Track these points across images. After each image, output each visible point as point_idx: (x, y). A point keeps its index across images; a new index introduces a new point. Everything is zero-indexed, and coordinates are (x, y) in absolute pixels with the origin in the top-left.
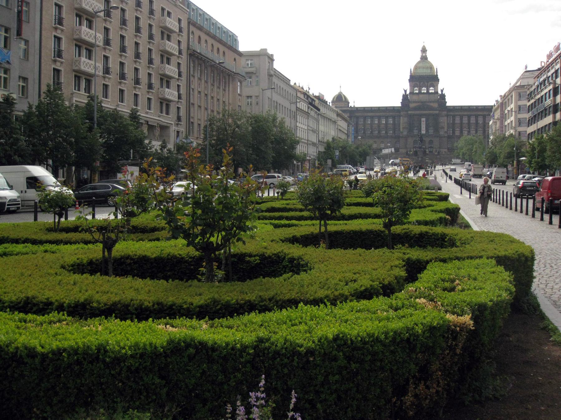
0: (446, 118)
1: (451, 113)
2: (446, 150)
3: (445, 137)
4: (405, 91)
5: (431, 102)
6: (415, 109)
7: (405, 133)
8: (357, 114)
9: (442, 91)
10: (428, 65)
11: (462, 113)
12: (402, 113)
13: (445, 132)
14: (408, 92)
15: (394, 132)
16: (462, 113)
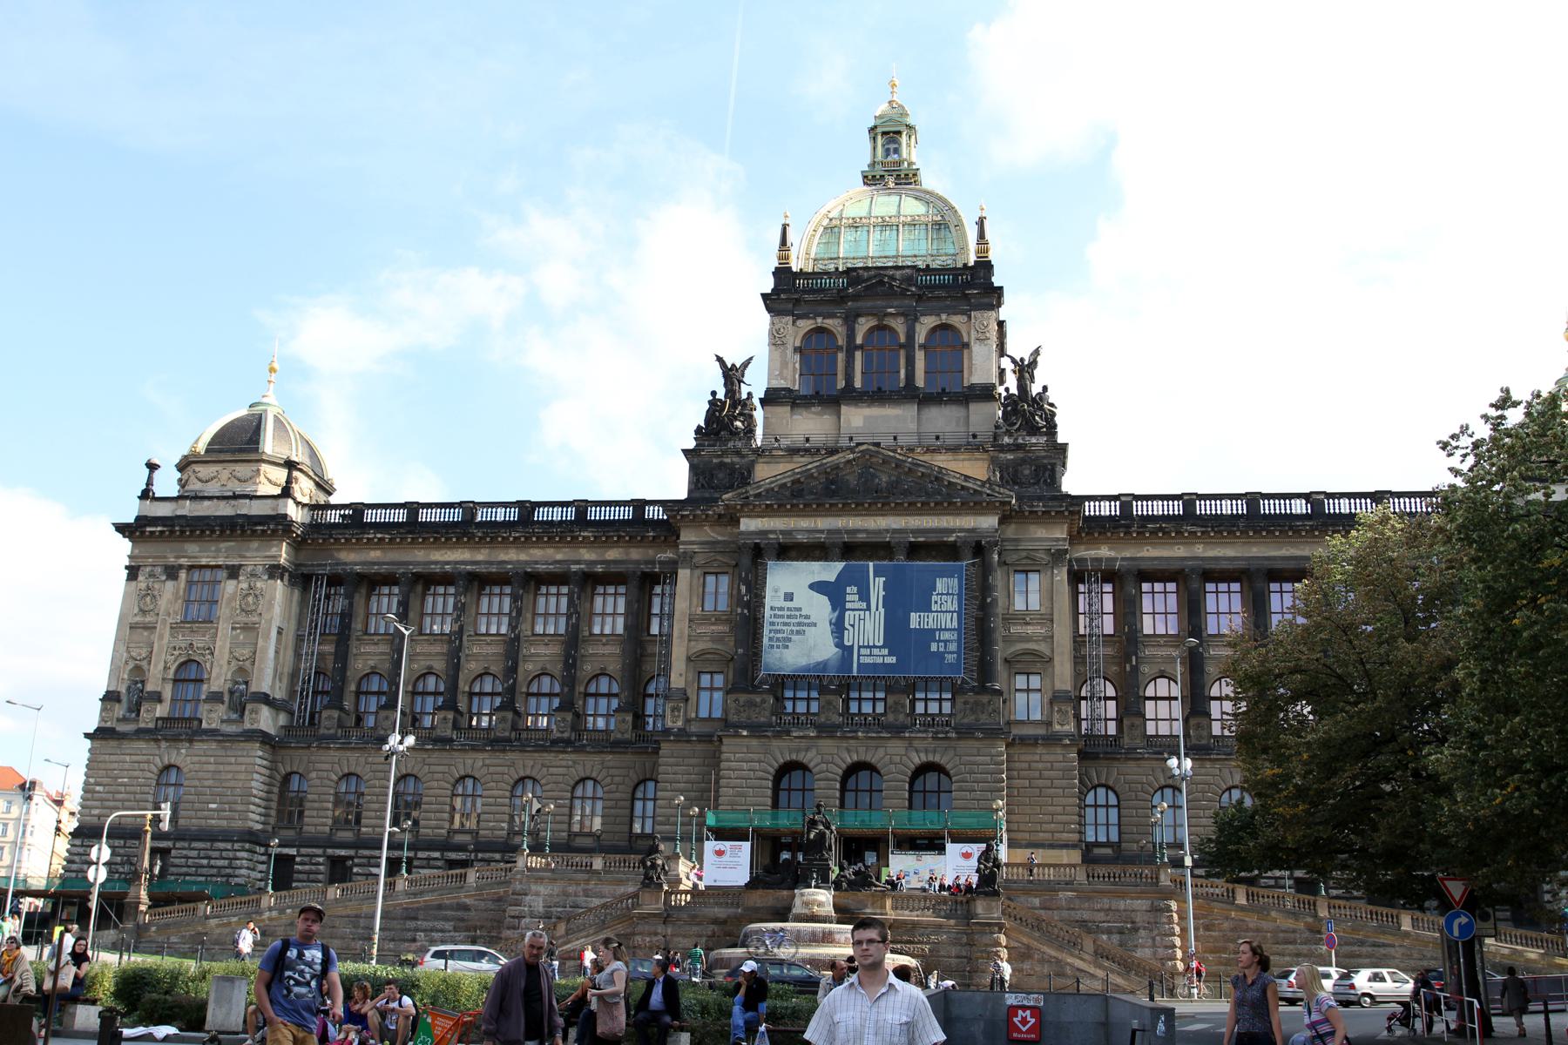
0: (1061, 575)
1: (1104, 552)
2: (1075, 856)
3: (1052, 740)
4: (732, 375)
5: (929, 450)
6: (793, 496)
7: (710, 704)
8: (353, 558)
9: (1025, 370)
10: (913, 208)
11: (1200, 550)
12: (687, 535)
13: (1057, 698)
14: (756, 384)
15: (634, 707)
16: (1200, 550)
